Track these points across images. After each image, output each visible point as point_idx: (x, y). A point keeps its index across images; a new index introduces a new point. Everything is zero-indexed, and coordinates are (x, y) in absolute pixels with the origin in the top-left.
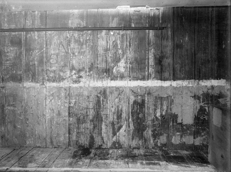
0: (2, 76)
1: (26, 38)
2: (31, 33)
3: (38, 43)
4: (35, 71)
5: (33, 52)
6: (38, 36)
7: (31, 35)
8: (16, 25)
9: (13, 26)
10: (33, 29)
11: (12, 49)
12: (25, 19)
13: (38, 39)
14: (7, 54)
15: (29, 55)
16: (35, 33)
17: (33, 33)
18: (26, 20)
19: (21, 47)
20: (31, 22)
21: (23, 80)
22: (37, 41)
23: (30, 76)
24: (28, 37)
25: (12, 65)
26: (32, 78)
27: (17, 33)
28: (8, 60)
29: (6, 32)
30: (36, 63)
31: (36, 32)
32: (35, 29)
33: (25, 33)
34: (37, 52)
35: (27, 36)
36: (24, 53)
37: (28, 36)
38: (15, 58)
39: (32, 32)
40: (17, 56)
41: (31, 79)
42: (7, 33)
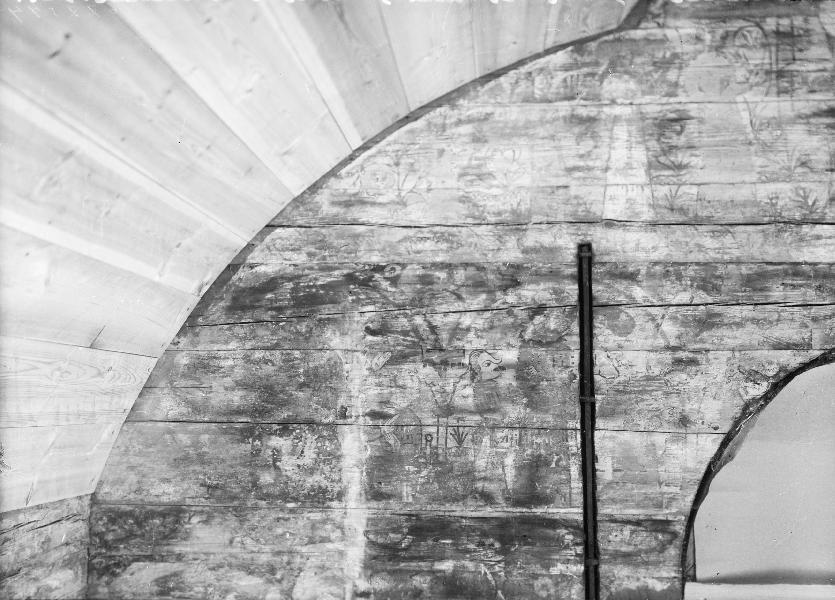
0: (392, 412)
1: (553, 523)
2: (577, 544)
3: (535, 577)
4: (412, 559)
5: (498, 552)
6: (563, 576)
7: (567, 547)
8: (610, 485)
9: (605, 467)
10: (597, 555)
11: (509, 461)
12: (638, 523)
13: (551, 577)
14: (486, 440)
15: (485, 534)
16: (576, 563)
17: (577, 555)
18: (633, 528)
19: (518, 503)
20: (624, 549)
21: (374, 504)
22: (544, 572)
23: (392, 535)
24: (558, 531)
25: (441, 458)
26: (384, 547)
27: (577, 485)
28: (460, 441)
29: (579, 436)
30: (447, 566)
31: (581, 568)
32: (596, 567)
33: (576, 521)
34: (497, 568)
35: (566, 528)
36: (488, 511)
37: (563, 531)
38: (469, 473)
39: (580, 550)
40: (479, 485)
41: (380, 540)
42: (575, 443)
